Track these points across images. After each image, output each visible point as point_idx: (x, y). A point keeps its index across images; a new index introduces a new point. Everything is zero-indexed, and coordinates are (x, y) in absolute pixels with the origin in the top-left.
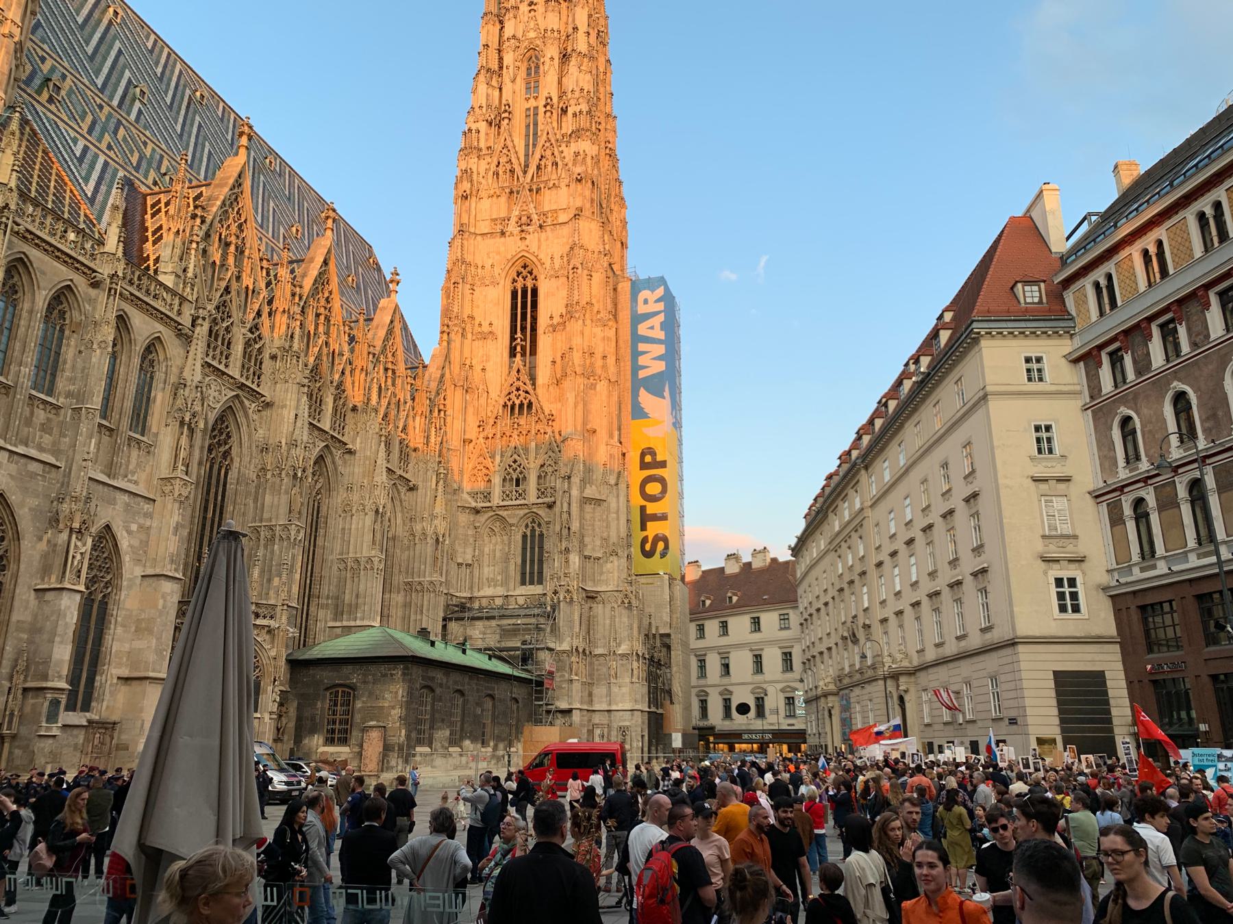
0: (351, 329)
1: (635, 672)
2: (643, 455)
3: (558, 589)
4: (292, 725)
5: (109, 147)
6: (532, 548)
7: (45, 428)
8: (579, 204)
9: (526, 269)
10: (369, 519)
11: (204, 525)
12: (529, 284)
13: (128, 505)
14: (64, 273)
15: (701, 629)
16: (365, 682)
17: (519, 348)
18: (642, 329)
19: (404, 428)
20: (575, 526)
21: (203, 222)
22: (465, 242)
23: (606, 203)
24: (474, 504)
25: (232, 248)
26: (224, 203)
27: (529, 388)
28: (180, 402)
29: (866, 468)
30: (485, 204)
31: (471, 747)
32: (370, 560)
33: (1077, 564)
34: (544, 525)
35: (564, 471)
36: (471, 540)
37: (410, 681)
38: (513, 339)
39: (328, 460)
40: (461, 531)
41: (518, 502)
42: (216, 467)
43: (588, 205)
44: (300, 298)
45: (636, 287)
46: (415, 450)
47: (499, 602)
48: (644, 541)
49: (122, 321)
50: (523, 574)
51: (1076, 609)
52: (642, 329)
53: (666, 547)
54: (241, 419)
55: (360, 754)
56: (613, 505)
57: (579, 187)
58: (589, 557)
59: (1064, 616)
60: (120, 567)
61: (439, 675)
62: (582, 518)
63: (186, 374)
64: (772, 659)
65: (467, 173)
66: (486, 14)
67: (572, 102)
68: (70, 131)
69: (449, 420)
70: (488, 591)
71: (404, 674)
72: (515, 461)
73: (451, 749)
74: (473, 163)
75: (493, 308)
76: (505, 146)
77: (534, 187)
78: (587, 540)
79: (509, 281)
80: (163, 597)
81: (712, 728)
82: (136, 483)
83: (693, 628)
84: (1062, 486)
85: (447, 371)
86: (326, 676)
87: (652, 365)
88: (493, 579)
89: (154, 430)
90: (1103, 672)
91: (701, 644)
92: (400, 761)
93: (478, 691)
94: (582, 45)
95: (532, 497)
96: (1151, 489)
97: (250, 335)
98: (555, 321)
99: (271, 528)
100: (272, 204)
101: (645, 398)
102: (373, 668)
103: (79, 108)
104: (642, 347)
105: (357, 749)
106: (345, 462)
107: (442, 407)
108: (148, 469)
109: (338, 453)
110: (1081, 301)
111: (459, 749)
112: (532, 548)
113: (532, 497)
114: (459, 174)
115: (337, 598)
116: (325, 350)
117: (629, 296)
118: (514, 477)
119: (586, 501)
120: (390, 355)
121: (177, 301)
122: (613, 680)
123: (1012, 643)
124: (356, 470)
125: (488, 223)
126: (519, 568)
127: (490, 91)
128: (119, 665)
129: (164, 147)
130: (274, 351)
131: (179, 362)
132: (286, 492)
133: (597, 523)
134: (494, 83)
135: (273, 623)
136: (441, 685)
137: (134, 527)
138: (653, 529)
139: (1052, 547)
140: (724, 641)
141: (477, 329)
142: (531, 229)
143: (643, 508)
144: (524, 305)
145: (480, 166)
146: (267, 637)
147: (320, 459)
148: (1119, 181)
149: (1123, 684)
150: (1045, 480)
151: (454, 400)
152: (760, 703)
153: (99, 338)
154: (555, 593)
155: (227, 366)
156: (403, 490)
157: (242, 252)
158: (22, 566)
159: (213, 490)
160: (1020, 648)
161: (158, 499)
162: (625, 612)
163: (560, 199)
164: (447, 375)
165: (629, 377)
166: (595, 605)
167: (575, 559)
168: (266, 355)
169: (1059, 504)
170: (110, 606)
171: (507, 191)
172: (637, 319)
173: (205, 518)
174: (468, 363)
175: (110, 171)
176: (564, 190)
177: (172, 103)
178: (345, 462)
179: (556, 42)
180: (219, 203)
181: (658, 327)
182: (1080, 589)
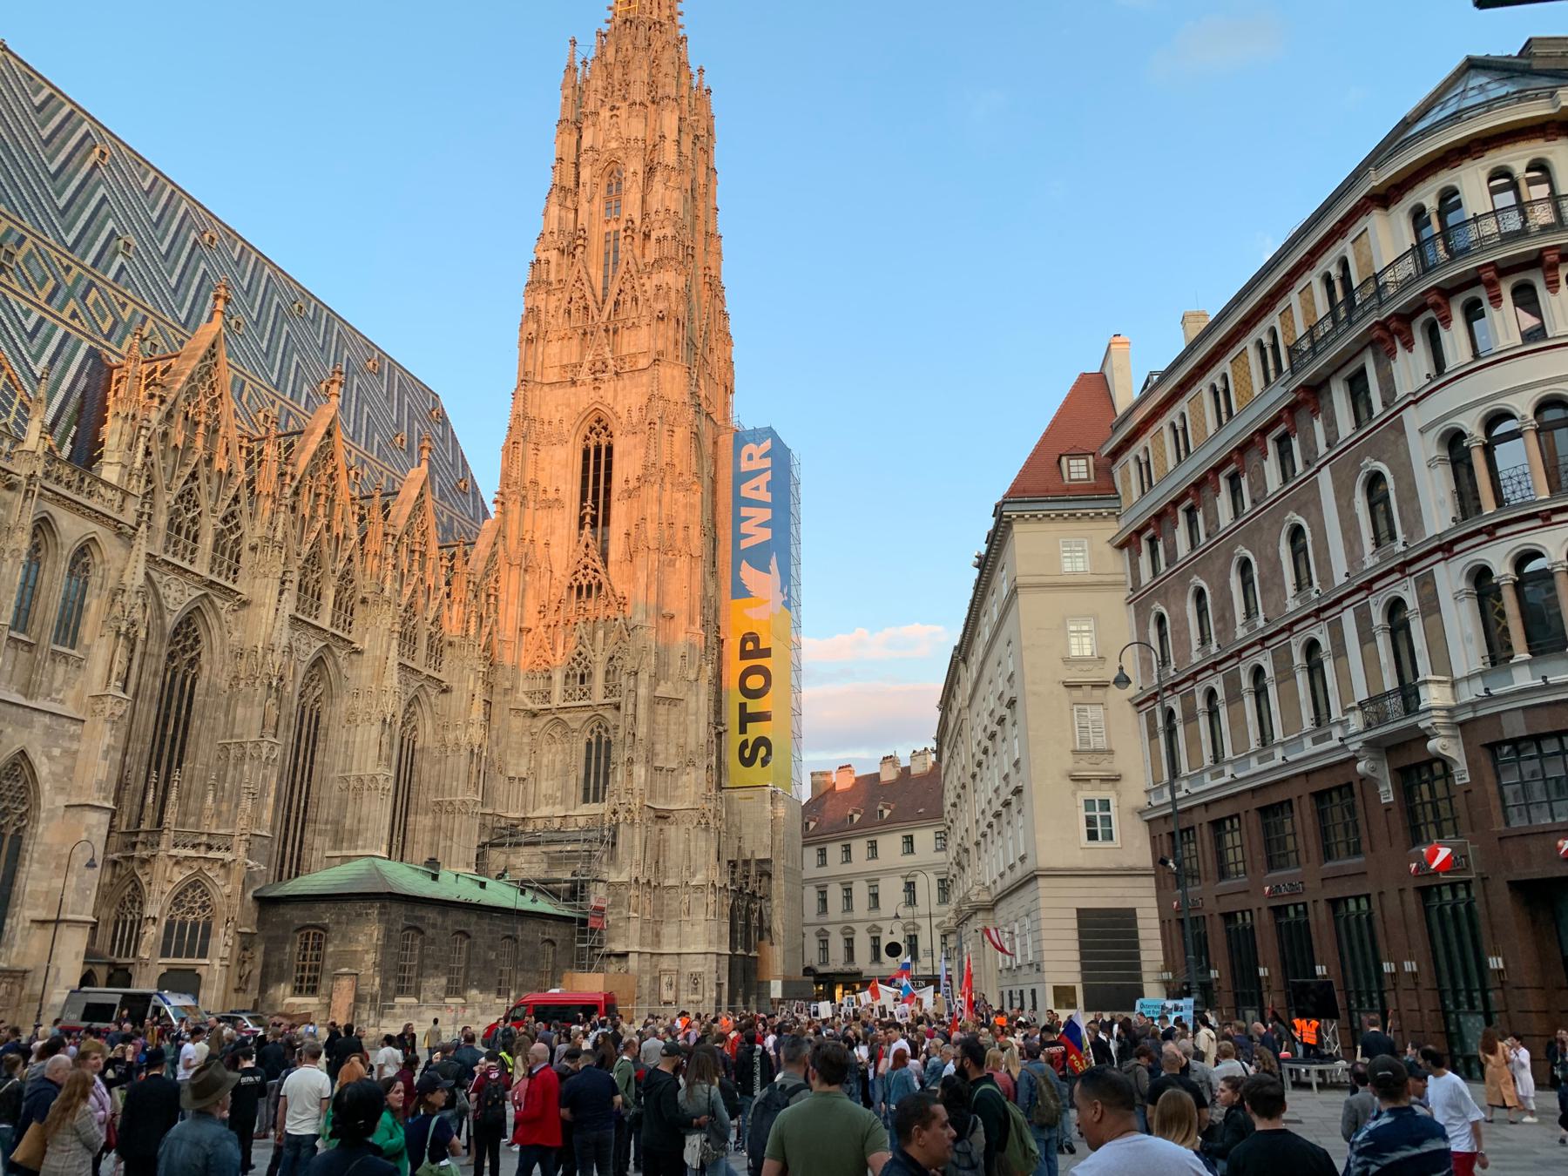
0: (362, 508)
1: (711, 908)
2: (744, 641)
3: (618, 808)
4: (257, 972)
5: (74, 315)
6: (598, 758)
8: (660, 347)
9: (600, 424)
10: (375, 730)
11: (162, 743)
12: (604, 442)
13: (49, 727)
15: (822, 853)
16: (338, 923)
17: (588, 519)
18: (746, 491)
19: (437, 619)
20: (642, 731)
21: (162, 401)
22: (529, 394)
23: (701, 340)
24: (530, 706)
25: (201, 429)
26: (191, 378)
27: (599, 565)
28: (117, 610)
29: (965, 660)
30: (554, 348)
31: (480, 997)
32: (374, 778)
33: (1110, 785)
34: (611, 731)
35: (630, 664)
36: (527, 749)
37: (387, 922)
38: (582, 508)
39: (330, 663)
40: (514, 738)
41: (582, 703)
42: (179, 677)
43: (671, 348)
44: (293, 478)
45: (740, 438)
46: (450, 644)
47: (557, 824)
48: (744, 745)
49: (44, 526)
50: (586, 790)
51: (1109, 836)
52: (746, 491)
53: (769, 753)
54: (211, 619)
55: (329, 1005)
56: (692, 705)
57: (662, 326)
58: (661, 769)
59: (1093, 844)
60: (37, 797)
61: (432, 915)
62: (652, 722)
63: (126, 579)
64: (927, 887)
65: (532, 313)
66: (561, 122)
67: (656, 225)
68: (22, 302)
69: (502, 605)
70: (545, 811)
71: (380, 914)
72: (580, 654)
73: (448, 1000)
74: (540, 299)
75: (560, 470)
76: (579, 279)
77: (611, 327)
78: (659, 747)
79: (579, 439)
81: (859, 974)
82: (62, 702)
83: (811, 854)
84: (1098, 692)
85: (500, 547)
86: (296, 915)
87: (756, 533)
88: (548, 793)
89: (86, 641)
90: (1134, 910)
91: (823, 872)
92: (372, 1014)
93: (491, 932)
94: (669, 156)
95: (598, 695)
96: (1178, 697)
97: (221, 526)
98: (631, 485)
99: (241, 745)
100: (296, 357)
101: (748, 573)
102: (347, 906)
103: (38, 275)
104: (745, 511)
105: (326, 1000)
106: (351, 663)
107: (492, 591)
108: (78, 685)
109: (341, 654)
110: (1126, 479)
111: (461, 1001)
112: (598, 758)
113: (598, 695)
114: (523, 311)
115: (337, 823)
116: (326, 535)
117: (731, 450)
118: (579, 673)
119: (657, 701)
120: (417, 535)
121: (119, 496)
122: (684, 918)
123: (1031, 878)
124: (364, 673)
125: (556, 370)
126: (581, 783)
127: (563, 213)
128: (35, 907)
129: (150, 306)
130: (255, 541)
131: (119, 564)
132: (260, 704)
133: (672, 727)
134: (569, 204)
135: (228, 857)
136: (434, 926)
137: (56, 752)
138: (755, 730)
139: (1084, 764)
140: (873, 865)
141: (541, 496)
142: (605, 376)
143: (743, 706)
144: (597, 467)
145: (551, 304)
146: (222, 872)
147: (319, 662)
148: (1186, 336)
149: (1156, 923)
150: (1078, 686)
151: (510, 582)
152: (913, 942)
153: (12, 545)
154: (615, 813)
155: (192, 562)
156: (433, 692)
157: (216, 431)
159: (174, 704)
160: (1041, 882)
161: (88, 719)
162: (702, 835)
163: (639, 341)
164: (501, 553)
165: (729, 548)
166: (666, 827)
167: (640, 771)
168: (245, 546)
169: (1094, 713)
170: (25, 841)
171: (580, 331)
172: (740, 478)
173: (164, 735)
174: (528, 537)
175: (70, 343)
176: (644, 332)
177: (168, 252)
178: (351, 663)
179: (641, 153)
180: (184, 378)
181: (763, 487)
182: (1113, 813)
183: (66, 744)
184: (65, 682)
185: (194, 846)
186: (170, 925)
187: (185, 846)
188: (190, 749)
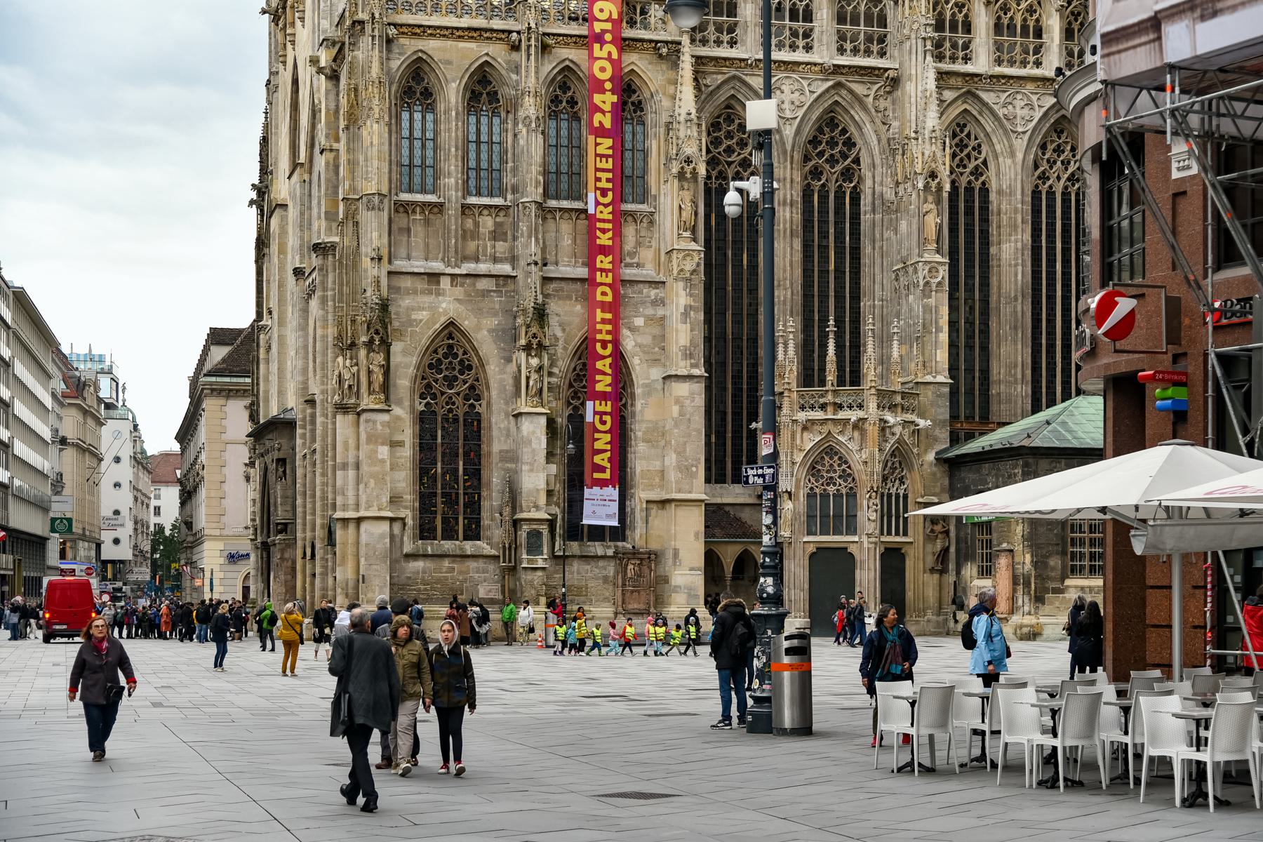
7: (496, 235)
14: (474, 51)
54: (859, 115)
80: (677, 401)
108: (654, 243)
158: (494, 393)
183: (650, 311)
184: (639, 244)
185: (823, 407)
186: (811, 496)
187: (812, 408)
188: (865, 283)
